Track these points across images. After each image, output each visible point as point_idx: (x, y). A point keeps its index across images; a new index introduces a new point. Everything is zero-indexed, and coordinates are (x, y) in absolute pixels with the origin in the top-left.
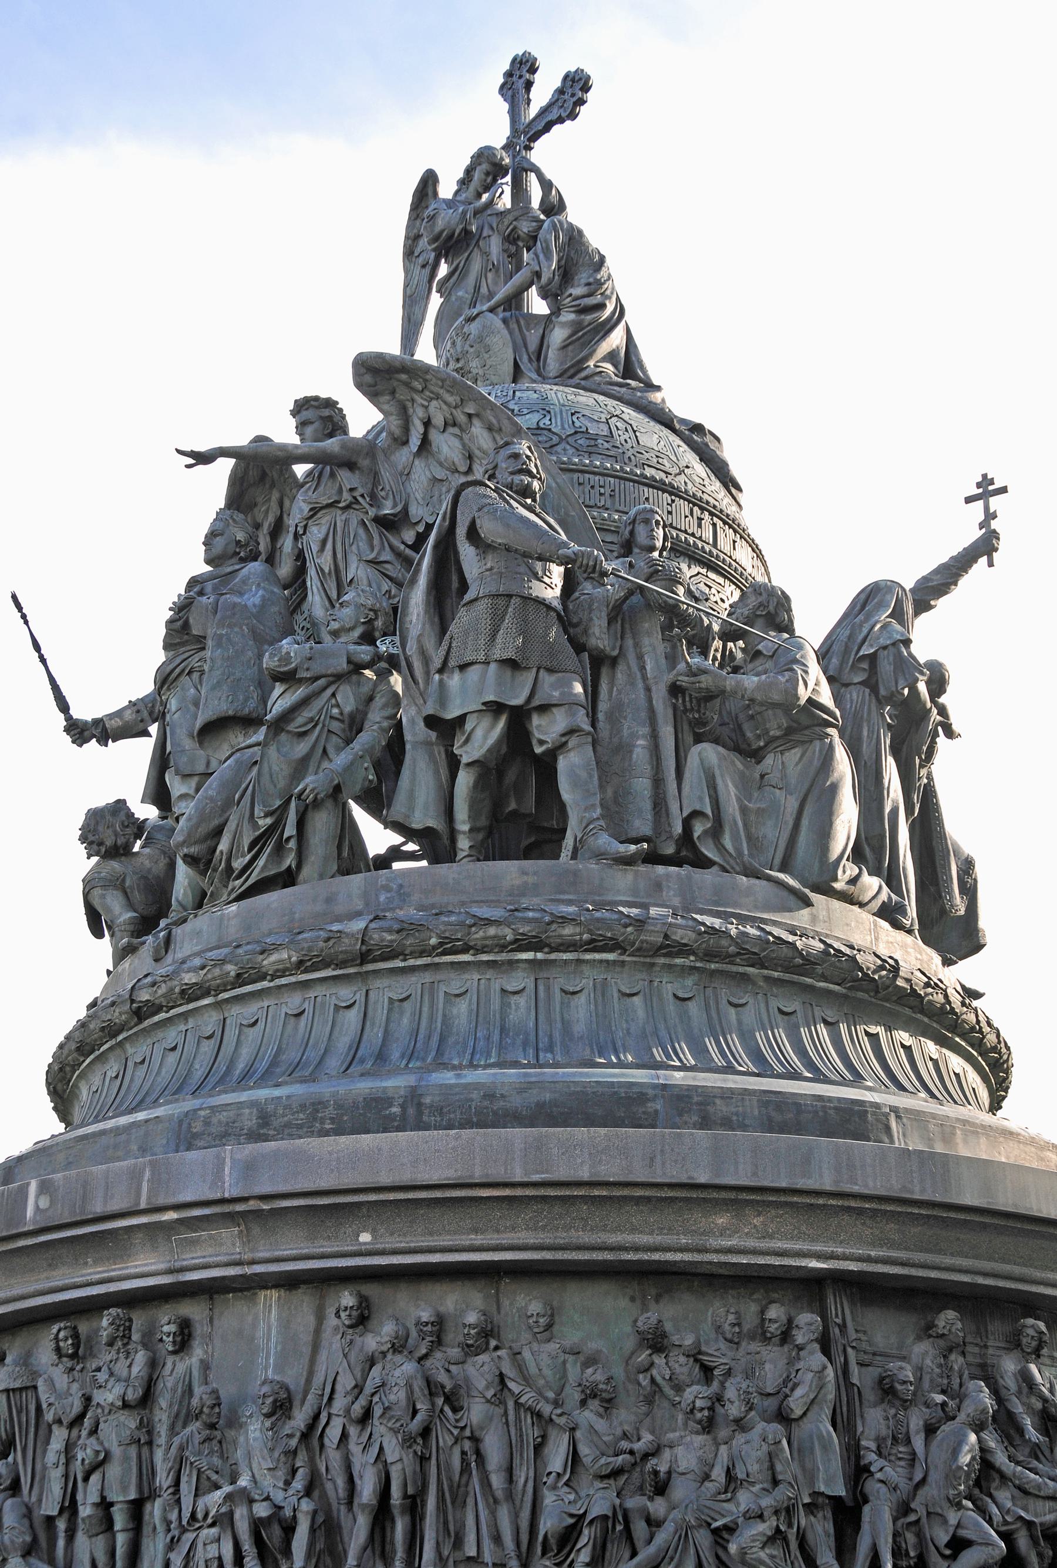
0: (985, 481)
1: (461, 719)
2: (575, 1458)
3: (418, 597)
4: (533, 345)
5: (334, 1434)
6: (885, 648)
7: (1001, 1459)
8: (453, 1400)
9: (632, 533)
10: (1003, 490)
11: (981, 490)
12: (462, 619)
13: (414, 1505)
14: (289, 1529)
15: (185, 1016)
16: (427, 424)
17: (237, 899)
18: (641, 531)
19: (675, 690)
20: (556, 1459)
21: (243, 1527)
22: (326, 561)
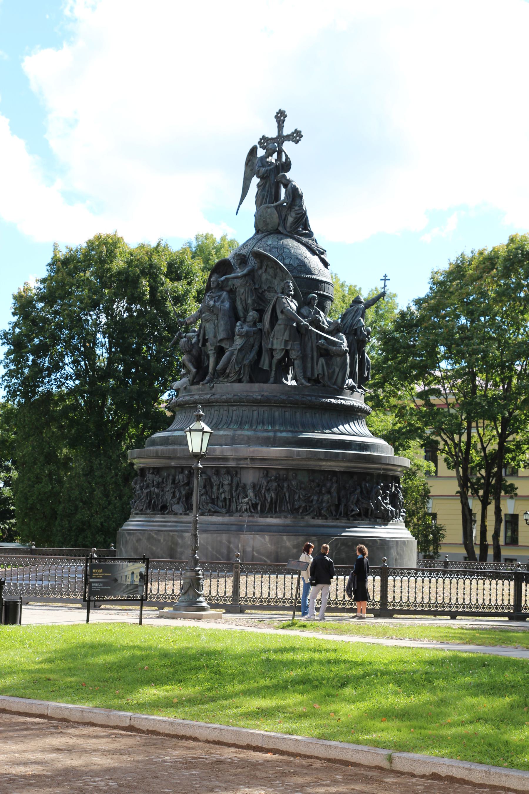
0: (385, 276)
1: (276, 349)
2: (299, 497)
3: (267, 317)
4: (283, 218)
5: (263, 491)
6: (359, 327)
7: (360, 499)
8: (282, 489)
9: (310, 301)
10: (389, 280)
11: (384, 278)
12: (277, 328)
13: (276, 503)
14: (257, 504)
15: (220, 405)
16: (267, 266)
17: (230, 383)
18: (312, 301)
19: (318, 347)
20: (296, 498)
21: (251, 504)
22: (243, 297)
